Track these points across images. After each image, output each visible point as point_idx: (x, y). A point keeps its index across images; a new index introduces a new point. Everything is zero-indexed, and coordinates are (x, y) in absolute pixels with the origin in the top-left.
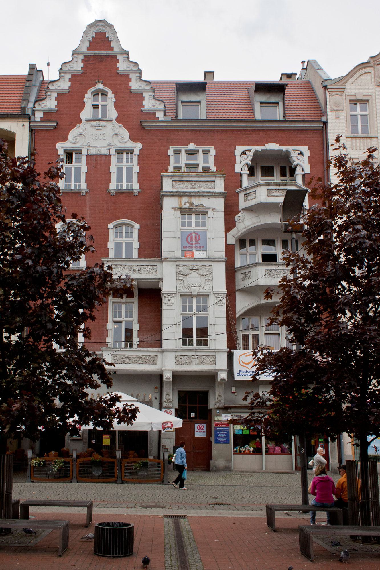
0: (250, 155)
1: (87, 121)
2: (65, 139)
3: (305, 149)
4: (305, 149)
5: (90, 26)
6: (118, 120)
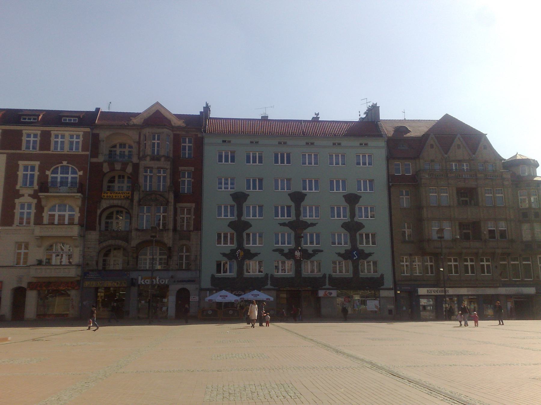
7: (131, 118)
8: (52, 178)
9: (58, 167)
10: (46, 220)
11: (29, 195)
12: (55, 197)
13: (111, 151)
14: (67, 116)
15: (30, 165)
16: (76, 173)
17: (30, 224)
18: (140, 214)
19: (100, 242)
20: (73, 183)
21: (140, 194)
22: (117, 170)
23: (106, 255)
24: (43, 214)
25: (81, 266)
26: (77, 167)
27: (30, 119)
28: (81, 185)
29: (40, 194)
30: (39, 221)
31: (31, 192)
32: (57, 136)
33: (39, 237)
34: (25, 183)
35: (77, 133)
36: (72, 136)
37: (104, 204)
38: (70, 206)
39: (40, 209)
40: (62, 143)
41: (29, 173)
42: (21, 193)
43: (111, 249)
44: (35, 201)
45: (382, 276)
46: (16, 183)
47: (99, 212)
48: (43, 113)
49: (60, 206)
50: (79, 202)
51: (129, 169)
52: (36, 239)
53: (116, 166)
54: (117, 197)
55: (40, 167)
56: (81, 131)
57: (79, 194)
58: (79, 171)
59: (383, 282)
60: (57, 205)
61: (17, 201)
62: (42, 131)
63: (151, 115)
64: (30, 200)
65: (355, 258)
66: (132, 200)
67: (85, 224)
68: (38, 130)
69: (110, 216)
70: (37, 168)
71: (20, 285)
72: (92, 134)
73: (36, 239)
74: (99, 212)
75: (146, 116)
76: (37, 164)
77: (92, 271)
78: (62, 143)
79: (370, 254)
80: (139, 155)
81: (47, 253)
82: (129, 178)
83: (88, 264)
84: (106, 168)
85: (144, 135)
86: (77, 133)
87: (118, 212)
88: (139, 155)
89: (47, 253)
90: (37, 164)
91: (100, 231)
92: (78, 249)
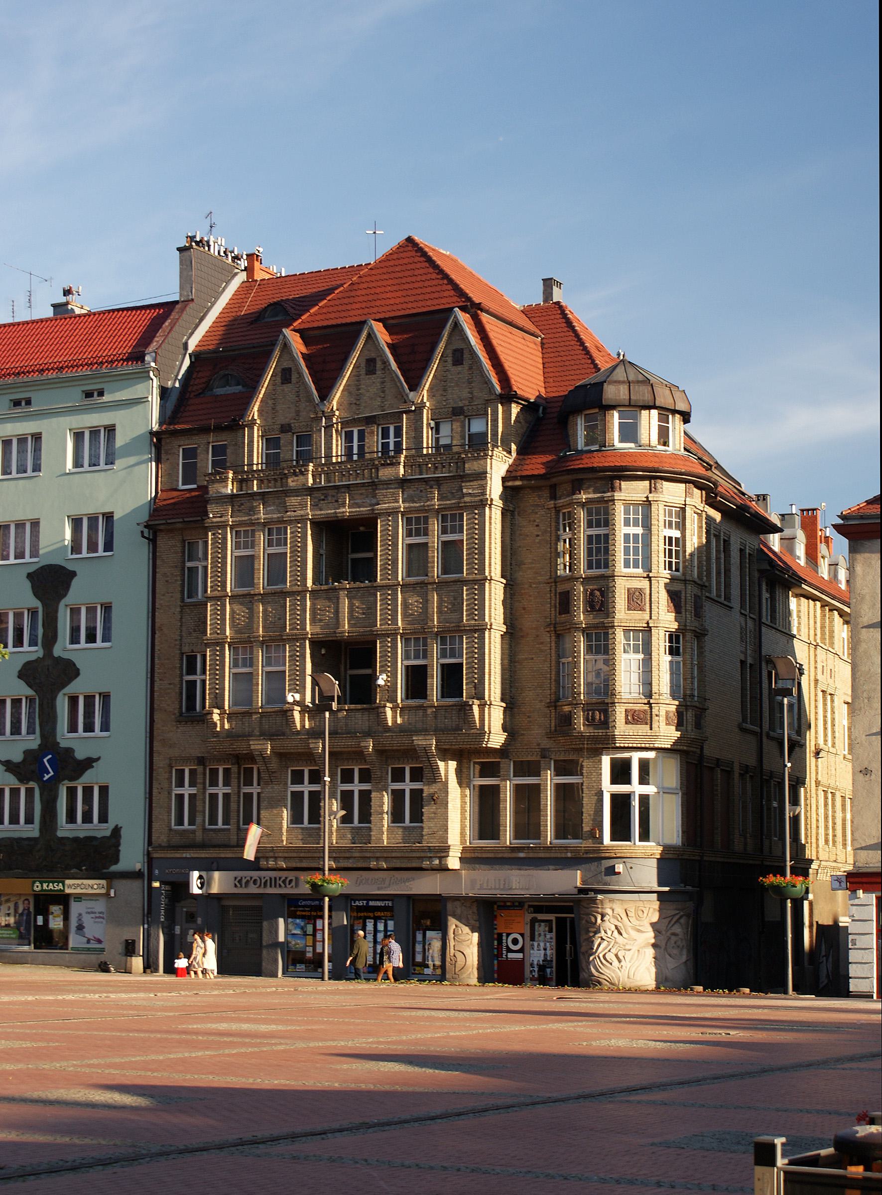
45: (117, 831)
59: (118, 852)
65: (46, 777)
79: (89, 763)
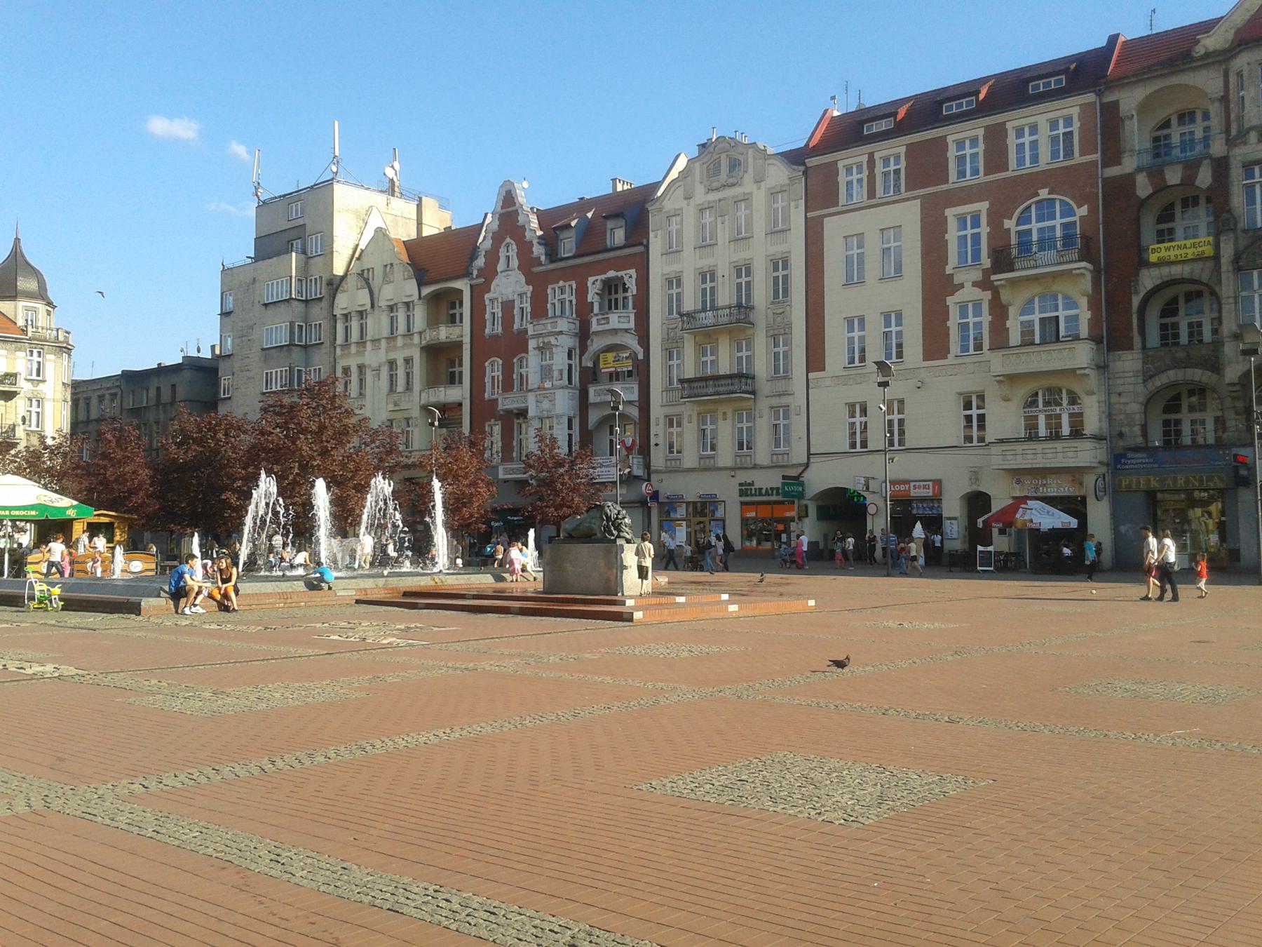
0: (598, 283)
1: (501, 272)
2: (489, 291)
3: (633, 272)
4: (633, 272)
5: (501, 187)
6: (519, 268)
7: (1198, 37)
8: (1019, 233)
9: (1029, 207)
10: (1015, 337)
11: (975, 284)
12: (1028, 279)
13: (1156, 139)
14: (1039, 77)
15: (968, 213)
16: (1072, 214)
17: (902, 358)
18: (1243, 294)
19: (1147, 378)
20: (1068, 239)
21: (1236, 239)
22: (1172, 186)
23: (1173, 406)
24: (1008, 324)
25: (1105, 439)
26: (1073, 198)
27: (960, 105)
28: (1088, 242)
29: (993, 278)
30: (1000, 341)
31: (977, 275)
32: (1020, 132)
33: (1001, 378)
34: (962, 256)
35: (1065, 112)
36: (1054, 124)
37: (1148, 279)
38: (1066, 297)
39: (999, 311)
40: (1034, 144)
41: (969, 232)
42: (957, 280)
43: (1179, 394)
44: (987, 295)
46: (944, 260)
47: (1136, 301)
48: (990, 83)
49: (1043, 298)
50: (1087, 284)
51: (1204, 178)
52: (998, 381)
53: (1168, 177)
54: (1179, 258)
55: (990, 213)
56: (1072, 107)
57: (1083, 264)
58: (1080, 206)
60: (1037, 299)
61: (950, 301)
62: (987, 128)
63: (1252, 13)
64: (978, 294)
66: (1216, 258)
67: (1105, 335)
68: (976, 129)
69: (1170, 310)
70: (984, 220)
71: (975, 488)
72: (1102, 105)
73: (998, 381)
74: (1136, 301)
75: (1240, 19)
76: (983, 207)
77: (1136, 449)
78: (1034, 144)
80: (1227, 131)
81: (1025, 412)
82: (1209, 200)
83: (1121, 435)
84: (1143, 187)
85: (1238, 74)
86: (1065, 112)
87: (1189, 297)
88: (1227, 131)
89: (1025, 412)
90: (983, 207)
91: (1144, 347)
92: (1094, 398)
